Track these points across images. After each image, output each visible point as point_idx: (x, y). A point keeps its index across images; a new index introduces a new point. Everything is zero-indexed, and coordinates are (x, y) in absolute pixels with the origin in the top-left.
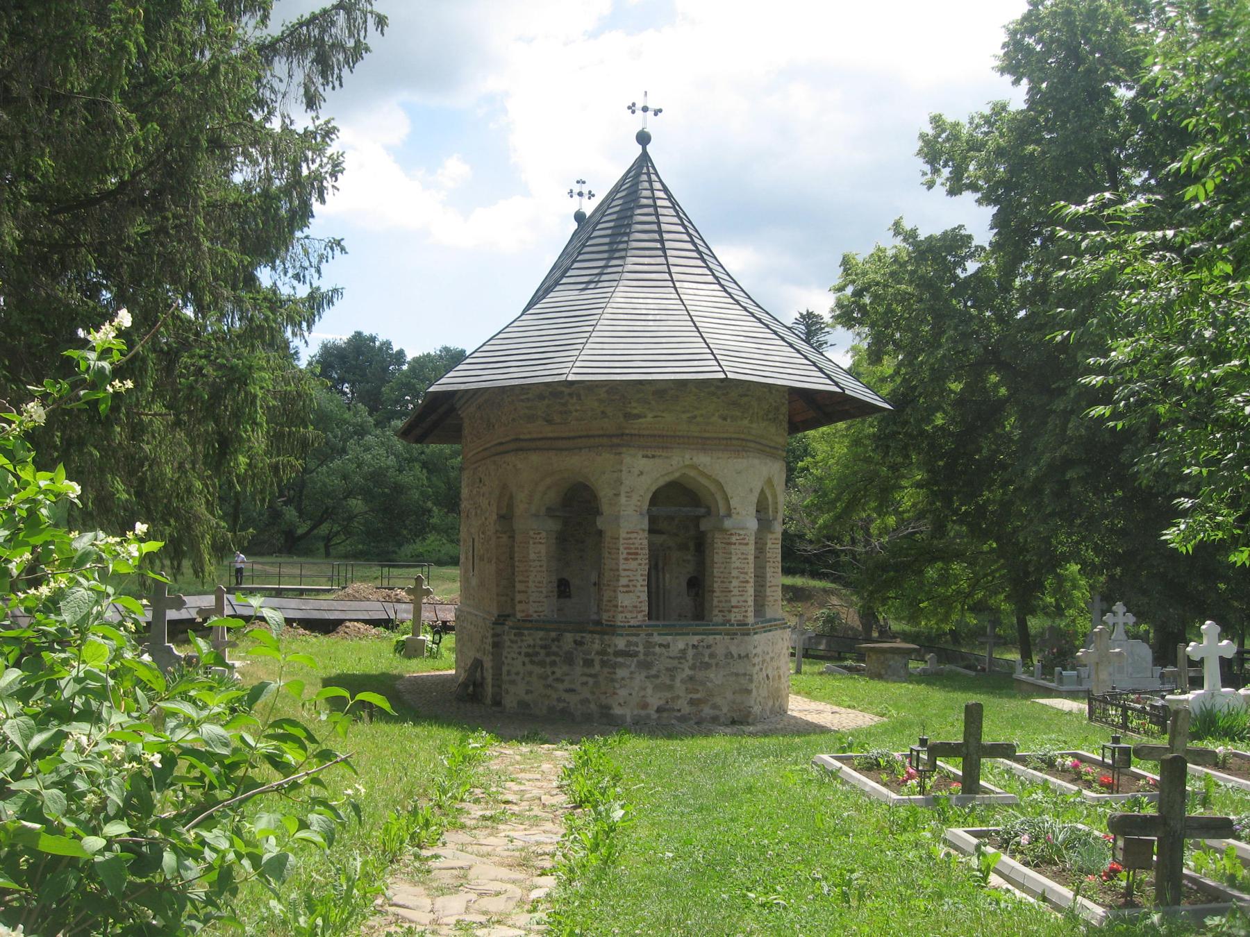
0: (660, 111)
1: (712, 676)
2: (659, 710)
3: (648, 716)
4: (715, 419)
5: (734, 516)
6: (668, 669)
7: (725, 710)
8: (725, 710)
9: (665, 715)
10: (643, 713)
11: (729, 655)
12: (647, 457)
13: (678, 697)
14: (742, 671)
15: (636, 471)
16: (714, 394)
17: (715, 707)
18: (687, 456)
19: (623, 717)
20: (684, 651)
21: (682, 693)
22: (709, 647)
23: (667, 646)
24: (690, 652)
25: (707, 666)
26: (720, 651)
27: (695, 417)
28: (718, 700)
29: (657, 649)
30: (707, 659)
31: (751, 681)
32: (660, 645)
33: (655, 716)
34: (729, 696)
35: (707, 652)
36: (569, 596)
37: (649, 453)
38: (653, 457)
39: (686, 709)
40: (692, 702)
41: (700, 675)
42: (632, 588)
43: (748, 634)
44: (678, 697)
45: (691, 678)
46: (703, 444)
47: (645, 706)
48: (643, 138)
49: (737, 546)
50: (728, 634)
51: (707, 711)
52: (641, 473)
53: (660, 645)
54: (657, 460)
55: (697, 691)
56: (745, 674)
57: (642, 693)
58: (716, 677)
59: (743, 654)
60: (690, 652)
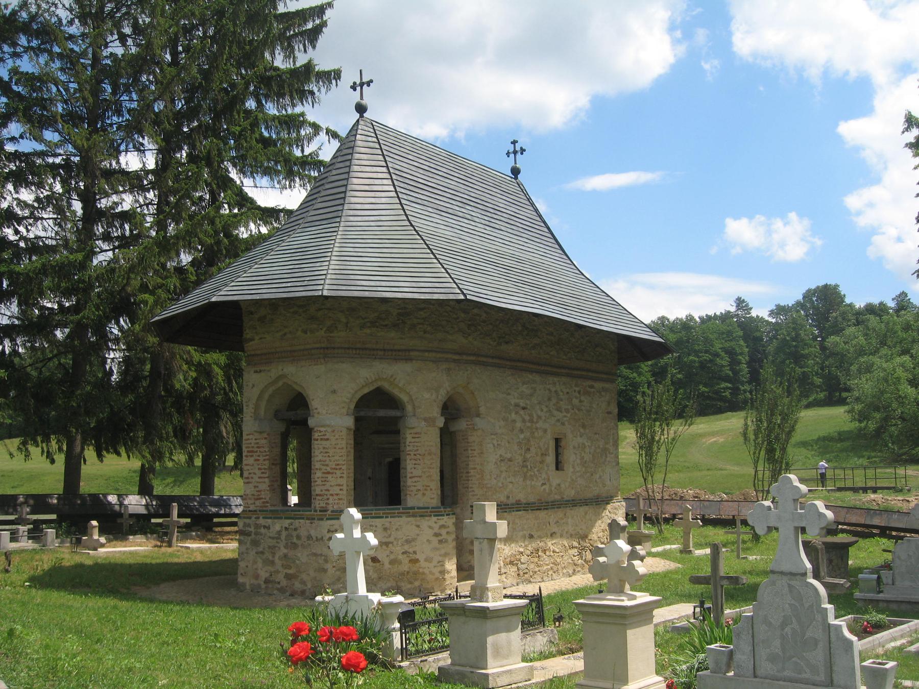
0: (371, 81)
1: (299, 555)
2: (267, 581)
3: (259, 585)
4: (299, 333)
5: (316, 415)
6: (269, 547)
7: (309, 586)
8: (309, 586)
9: (270, 586)
10: (256, 582)
11: (309, 537)
12: (256, 372)
13: (278, 572)
14: (319, 552)
15: (251, 385)
17: (304, 583)
18: (280, 368)
19: (244, 584)
20: (279, 533)
21: (280, 569)
22: (296, 529)
23: (268, 528)
24: (284, 534)
25: (295, 546)
26: (303, 533)
27: (285, 334)
28: (304, 576)
29: (263, 530)
30: (295, 540)
31: (326, 561)
32: (265, 527)
33: (263, 586)
35: (294, 534)
37: (258, 369)
38: (260, 371)
39: (284, 583)
40: (288, 577)
41: (291, 553)
42: (250, 480)
43: (322, 519)
44: (278, 572)
45: (285, 556)
46: (293, 356)
47: (257, 577)
48: (361, 109)
49: (319, 442)
50: (308, 519)
51: (298, 586)
52: (254, 386)
53: (265, 527)
54: (263, 374)
55: (290, 568)
56: (321, 555)
57: (255, 567)
58: (302, 556)
59: (319, 537)
60: (284, 534)
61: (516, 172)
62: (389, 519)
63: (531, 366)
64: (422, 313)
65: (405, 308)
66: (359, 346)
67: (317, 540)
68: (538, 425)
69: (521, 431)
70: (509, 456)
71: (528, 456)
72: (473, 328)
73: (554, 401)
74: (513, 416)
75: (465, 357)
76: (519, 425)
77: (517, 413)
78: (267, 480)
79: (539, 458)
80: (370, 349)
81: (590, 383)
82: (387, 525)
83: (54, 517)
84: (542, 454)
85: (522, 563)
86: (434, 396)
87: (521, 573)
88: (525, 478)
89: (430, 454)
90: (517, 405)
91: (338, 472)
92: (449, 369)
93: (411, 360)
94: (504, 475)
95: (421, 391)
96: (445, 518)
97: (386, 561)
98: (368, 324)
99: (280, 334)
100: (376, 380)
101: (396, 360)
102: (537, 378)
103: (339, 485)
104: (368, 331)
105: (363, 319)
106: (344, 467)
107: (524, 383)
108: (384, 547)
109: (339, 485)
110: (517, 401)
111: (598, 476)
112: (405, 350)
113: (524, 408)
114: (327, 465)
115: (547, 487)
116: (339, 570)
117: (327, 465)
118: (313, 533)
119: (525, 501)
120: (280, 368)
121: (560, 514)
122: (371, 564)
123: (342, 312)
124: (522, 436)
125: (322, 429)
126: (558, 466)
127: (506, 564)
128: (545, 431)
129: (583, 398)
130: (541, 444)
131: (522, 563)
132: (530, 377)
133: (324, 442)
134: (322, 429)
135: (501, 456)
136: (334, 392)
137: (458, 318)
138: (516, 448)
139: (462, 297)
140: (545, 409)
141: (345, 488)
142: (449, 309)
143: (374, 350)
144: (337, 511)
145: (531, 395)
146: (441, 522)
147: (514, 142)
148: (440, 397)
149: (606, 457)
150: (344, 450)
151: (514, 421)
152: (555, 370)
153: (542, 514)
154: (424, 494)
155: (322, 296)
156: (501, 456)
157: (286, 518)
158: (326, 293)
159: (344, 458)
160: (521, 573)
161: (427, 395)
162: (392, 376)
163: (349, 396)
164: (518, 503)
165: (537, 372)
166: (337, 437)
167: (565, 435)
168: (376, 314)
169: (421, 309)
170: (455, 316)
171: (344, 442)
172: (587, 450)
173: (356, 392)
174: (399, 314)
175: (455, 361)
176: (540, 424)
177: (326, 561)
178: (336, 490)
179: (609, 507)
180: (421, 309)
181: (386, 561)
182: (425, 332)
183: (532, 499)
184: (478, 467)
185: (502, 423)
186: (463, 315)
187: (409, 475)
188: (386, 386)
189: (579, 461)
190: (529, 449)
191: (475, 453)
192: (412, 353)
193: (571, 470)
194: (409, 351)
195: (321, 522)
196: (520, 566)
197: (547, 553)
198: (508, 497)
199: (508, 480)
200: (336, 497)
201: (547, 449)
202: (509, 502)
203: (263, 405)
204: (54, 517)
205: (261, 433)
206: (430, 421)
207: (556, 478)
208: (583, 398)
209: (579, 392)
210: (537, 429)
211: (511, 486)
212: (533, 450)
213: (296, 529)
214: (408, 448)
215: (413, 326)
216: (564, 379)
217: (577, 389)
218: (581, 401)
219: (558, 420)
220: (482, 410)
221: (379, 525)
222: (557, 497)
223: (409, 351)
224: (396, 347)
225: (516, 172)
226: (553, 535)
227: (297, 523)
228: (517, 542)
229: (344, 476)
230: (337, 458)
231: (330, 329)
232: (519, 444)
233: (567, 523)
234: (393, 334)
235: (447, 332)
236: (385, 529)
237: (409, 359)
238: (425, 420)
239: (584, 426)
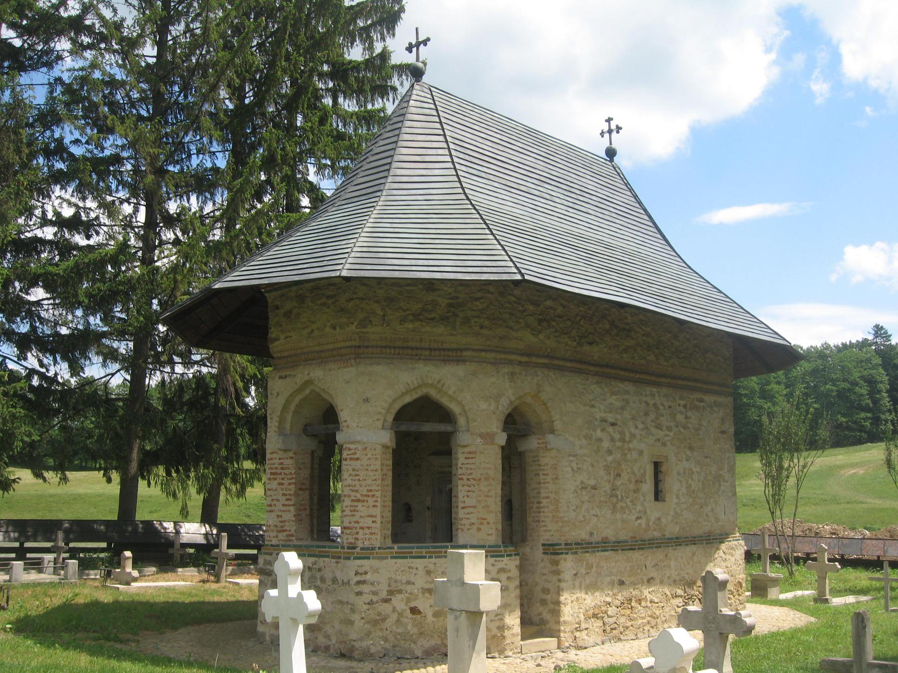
0: (428, 39)
4: (328, 330)
5: (345, 429)
8: (334, 641)
11: (335, 580)
12: (281, 378)
15: (276, 394)
16: (325, 304)
17: (327, 637)
18: (306, 372)
19: (263, 634)
22: (320, 570)
27: (312, 331)
28: (328, 629)
31: (353, 611)
34: (337, 625)
35: (318, 575)
36: (411, 521)
37: (283, 374)
38: (286, 377)
42: (273, 508)
43: (349, 558)
46: (322, 357)
49: (348, 462)
50: (333, 557)
54: (288, 380)
56: (347, 603)
59: (346, 580)
61: (611, 153)
62: (433, 560)
63: (622, 373)
64: (478, 303)
65: (457, 298)
66: (398, 344)
67: (343, 583)
68: (631, 446)
69: (610, 452)
70: (592, 482)
71: (618, 483)
72: (545, 324)
73: (652, 416)
74: (599, 433)
75: (534, 359)
76: (606, 444)
77: (603, 430)
78: (292, 508)
79: (632, 486)
80: (412, 349)
81: (698, 395)
82: (431, 567)
83: (104, 545)
84: (637, 481)
85: (609, 617)
86: (493, 407)
87: (608, 629)
88: (614, 510)
89: (487, 479)
90: (603, 420)
91: (369, 499)
92: (512, 374)
93: (464, 361)
95: (477, 400)
96: (506, 559)
97: (429, 613)
98: (411, 317)
99: (307, 331)
100: (419, 387)
101: (446, 361)
102: (630, 387)
103: (372, 516)
104: (411, 326)
105: (404, 311)
106: (378, 494)
107: (613, 394)
108: (427, 595)
109: (372, 516)
110: (603, 415)
111: (709, 508)
112: (457, 350)
113: (613, 424)
114: (357, 491)
115: (643, 522)
116: (368, 622)
117: (357, 491)
118: (339, 575)
119: (614, 540)
120: (306, 372)
121: (659, 554)
122: (410, 616)
123: (377, 302)
124: (610, 458)
125: (352, 446)
126: (658, 495)
127: (587, 618)
128: (641, 453)
129: (689, 414)
130: (636, 469)
131: (609, 617)
132: (622, 386)
133: (352, 462)
134: (352, 446)
135: (582, 482)
136: (367, 400)
137: (524, 311)
138: (602, 473)
139: (518, 277)
140: (641, 426)
141: (378, 519)
142: (513, 299)
143: (417, 349)
144: (368, 549)
145: (623, 408)
146: (500, 565)
147: (609, 120)
148: (500, 408)
149: (720, 486)
150: (379, 472)
151: (600, 440)
152: (653, 378)
153: (636, 555)
154: (479, 529)
155: (339, 277)
156: (582, 482)
157: (310, 556)
158: (345, 273)
159: (379, 482)
160: (608, 629)
161: (484, 406)
162: (439, 382)
163: (386, 405)
164: (605, 541)
165: (629, 380)
166: (369, 456)
167: (666, 458)
168: (420, 306)
169: (477, 299)
170: (520, 308)
171: (378, 463)
172: (696, 477)
173: (394, 401)
174: (450, 305)
175: (520, 363)
176: (635, 444)
177: (353, 611)
178: (368, 522)
179: (723, 546)
180: (477, 299)
181: (429, 613)
182: (482, 327)
183: (622, 536)
184: (553, 496)
185: (584, 442)
186: (531, 308)
187: (461, 505)
188: (433, 393)
189: (684, 490)
190: (619, 475)
191: (549, 478)
192: (464, 353)
193: (676, 501)
194: (461, 350)
195: (348, 562)
196: (606, 619)
197: (643, 604)
198: (591, 534)
199: (594, 512)
200: (367, 531)
201: (644, 475)
202: (593, 540)
203: (289, 417)
204: (104, 545)
205: (285, 451)
206: (488, 438)
207: (654, 511)
208: (689, 414)
209: (685, 406)
210: (629, 450)
211: (595, 519)
212: (625, 475)
213: (320, 570)
214: (460, 471)
215: (467, 320)
216: (665, 390)
217: (682, 402)
218: (686, 418)
219: (658, 440)
220: (558, 425)
221: (421, 568)
222: (657, 534)
223: (461, 350)
224: (446, 346)
225: (611, 153)
226: (650, 581)
227: (321, 562)
228: (603, 590)
229: (378, 504)
230: (369, 482)
231: (363, 324)
232: (607, 468)
233: (669, 567)
234: (441, 329)
235: (511, 328)
236: (429, 572)
237: (460, 361)
238: (481, 436)
239: (691, 448)
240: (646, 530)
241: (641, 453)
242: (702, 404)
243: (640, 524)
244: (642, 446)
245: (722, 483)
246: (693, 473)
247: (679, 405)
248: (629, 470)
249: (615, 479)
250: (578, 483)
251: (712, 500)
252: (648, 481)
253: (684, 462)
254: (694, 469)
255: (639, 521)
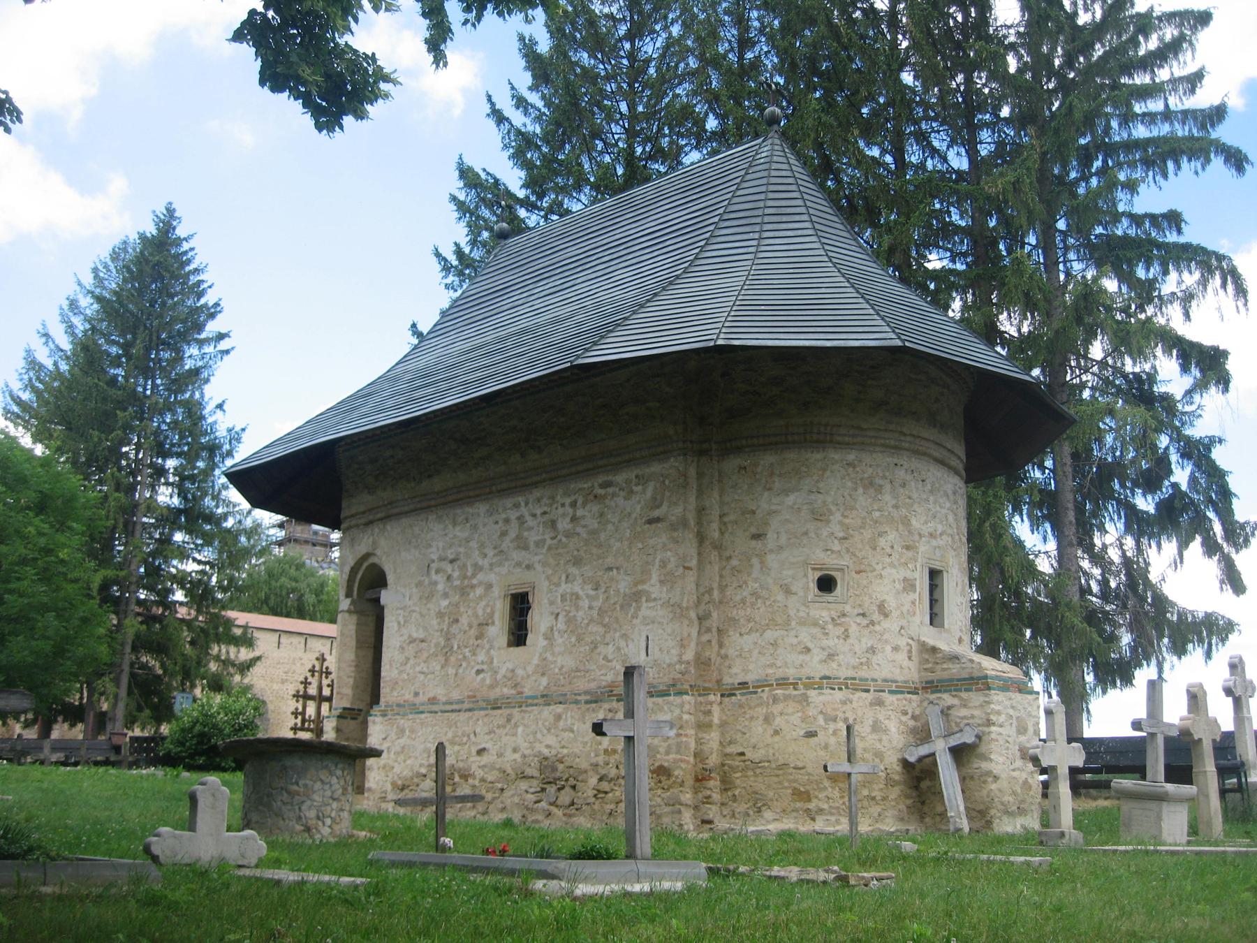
68: (475, 581)
69: (446, 595)
70: (422, 636)
71: (454, 629)
79: (473, 632)
94: (412, 662)
102: (482, 508)
113: (452, 561)
119: (444, 699)
128: (489, 586)
129: (579, 513)
130: (480, 612)
132: (471, 510)
140: (491, 553)
149: (639, 608)
151: (436, 583)
156: (410, 636)
164: (433, 701)
172: (585, 603)
176: (481, 576)
189: (561, 625)
190: (457, 621)
193: (542, 642)
197: (470, 781)
198: (416, 694)
199: (418, 669)
202: (418, 700)
207: (508, 659)
211: (422, 677)
212: (464, 620)
216: (537, 493)
217: (568, 501)
218: (574, 519)
219: (519, 564)
232: (440, 615)
239: (577, 562)
240: (492, 687)
241: (489, 586)
242: (610, 490)
243: (484, 680)
244: (492, 577)
245: (645, 605)
246: (578, 597)
247: (563, 505)
248: (470, 612)
249: (450, 625)
250: (406, 637)
251: (617, 634)
252: (497, 622)
253: (563, 586)
254: (581, 593)
255: (481, 676)
